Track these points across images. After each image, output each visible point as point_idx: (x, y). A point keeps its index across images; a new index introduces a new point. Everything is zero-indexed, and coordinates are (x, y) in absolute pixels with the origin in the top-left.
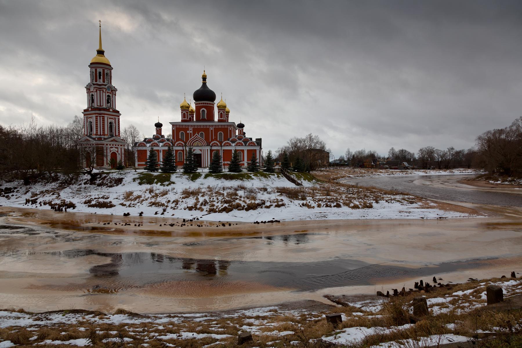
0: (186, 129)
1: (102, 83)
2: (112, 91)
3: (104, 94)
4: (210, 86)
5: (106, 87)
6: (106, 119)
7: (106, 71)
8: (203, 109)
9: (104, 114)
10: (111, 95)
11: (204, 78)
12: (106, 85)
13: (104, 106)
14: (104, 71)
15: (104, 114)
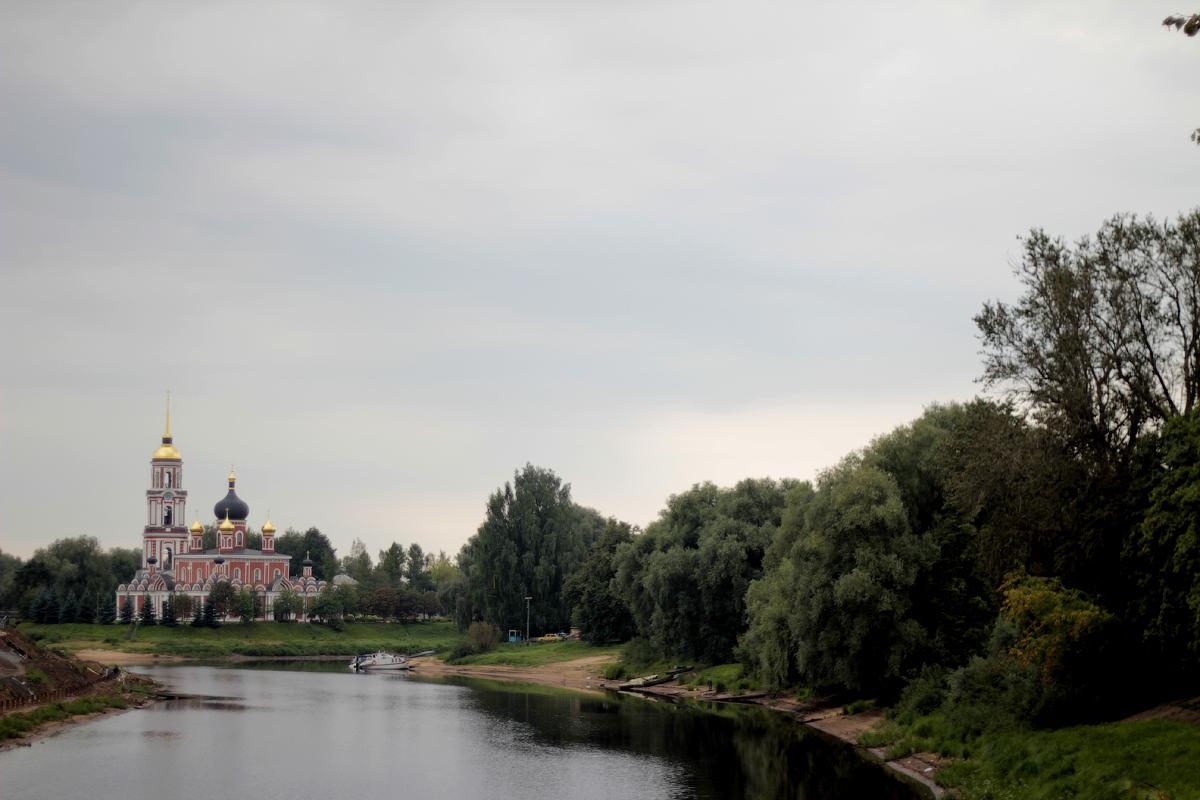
0: (187, 565)
1: (159, 489)
2: (174, 499)
3: (159, 506)
4: (241, 495)
5: (162, 495)
6: (158, 545)
7: (165, 470)
8: (240, 531)
9: (155, 537)
10: (172, 506)
11: (232, 484)
12: (160, 492)
13: (159, 525)
14: (162, 470)
15: (155, 537)
